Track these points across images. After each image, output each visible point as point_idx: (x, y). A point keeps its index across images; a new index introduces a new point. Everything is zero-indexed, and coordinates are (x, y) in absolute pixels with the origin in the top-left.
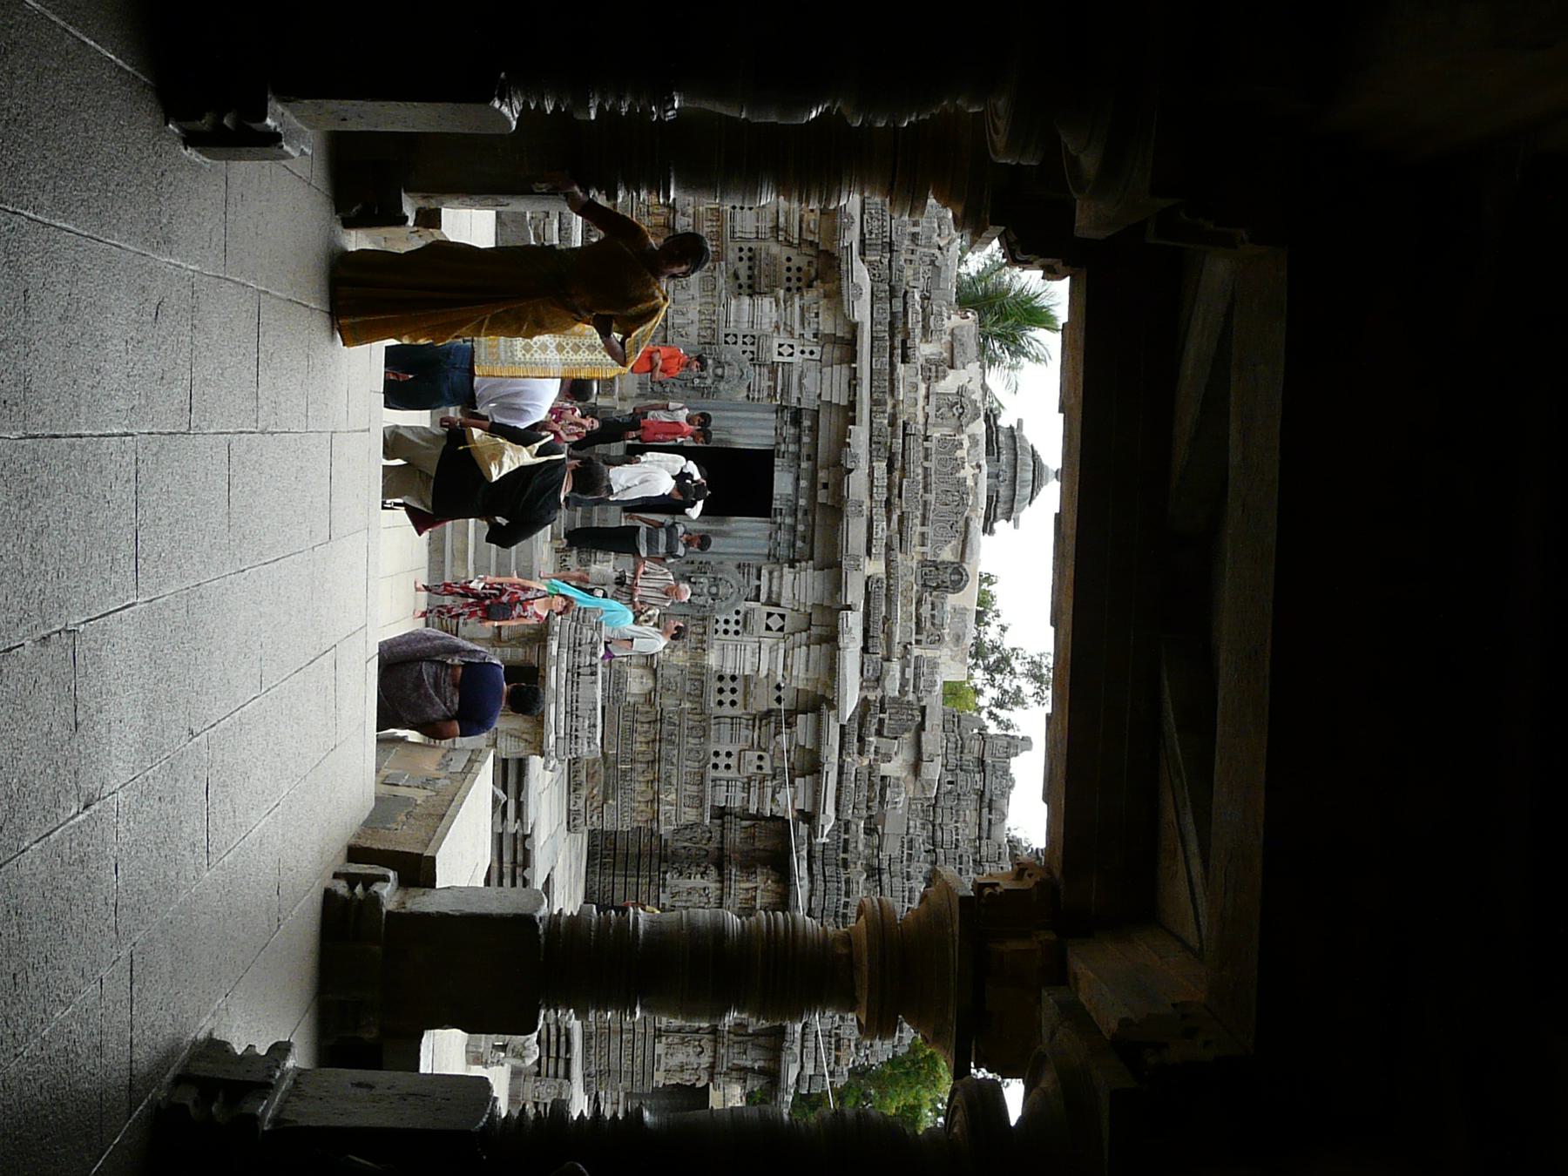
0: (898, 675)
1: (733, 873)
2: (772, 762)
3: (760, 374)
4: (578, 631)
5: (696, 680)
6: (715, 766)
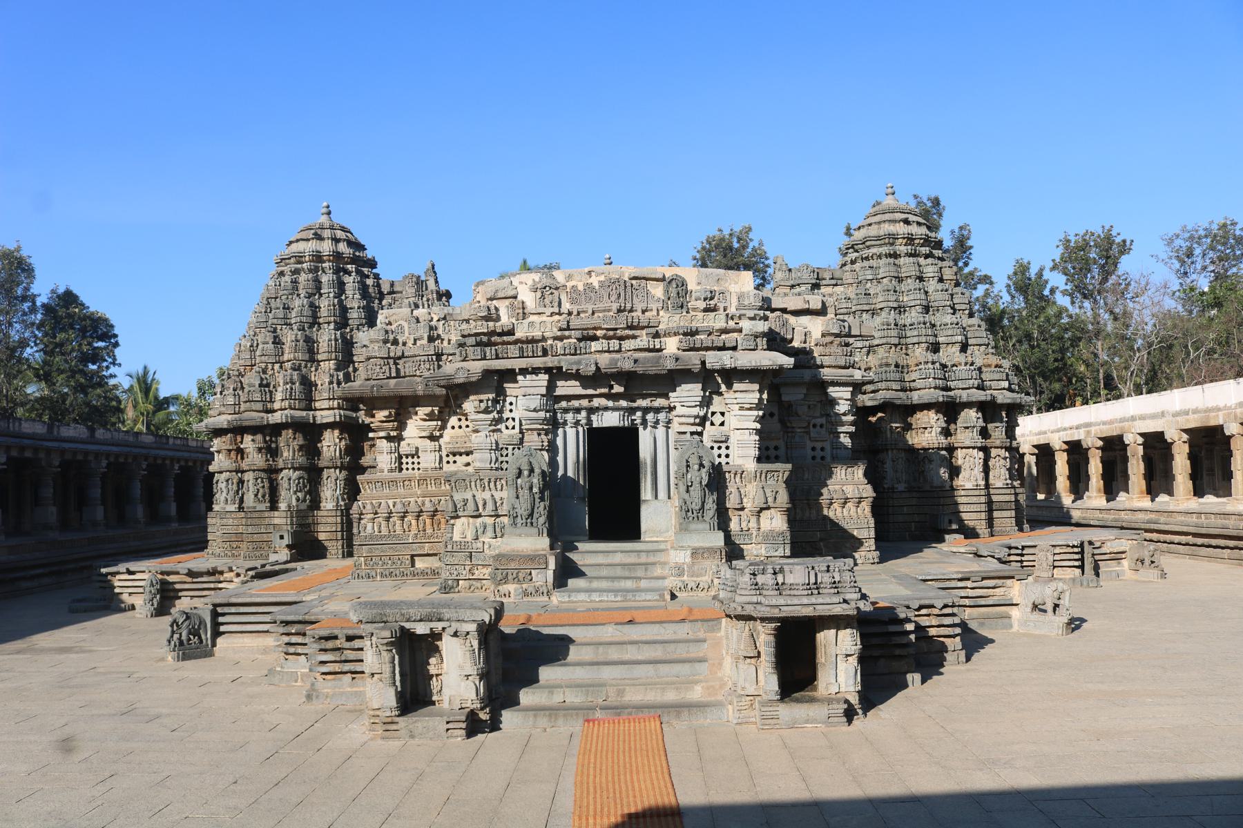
0: (753, 322)
1: (879, 442)
2: (817, 417)
3: (528, 442)
4: (744, 586)
5: (766, 478)
6: (823, 458)
